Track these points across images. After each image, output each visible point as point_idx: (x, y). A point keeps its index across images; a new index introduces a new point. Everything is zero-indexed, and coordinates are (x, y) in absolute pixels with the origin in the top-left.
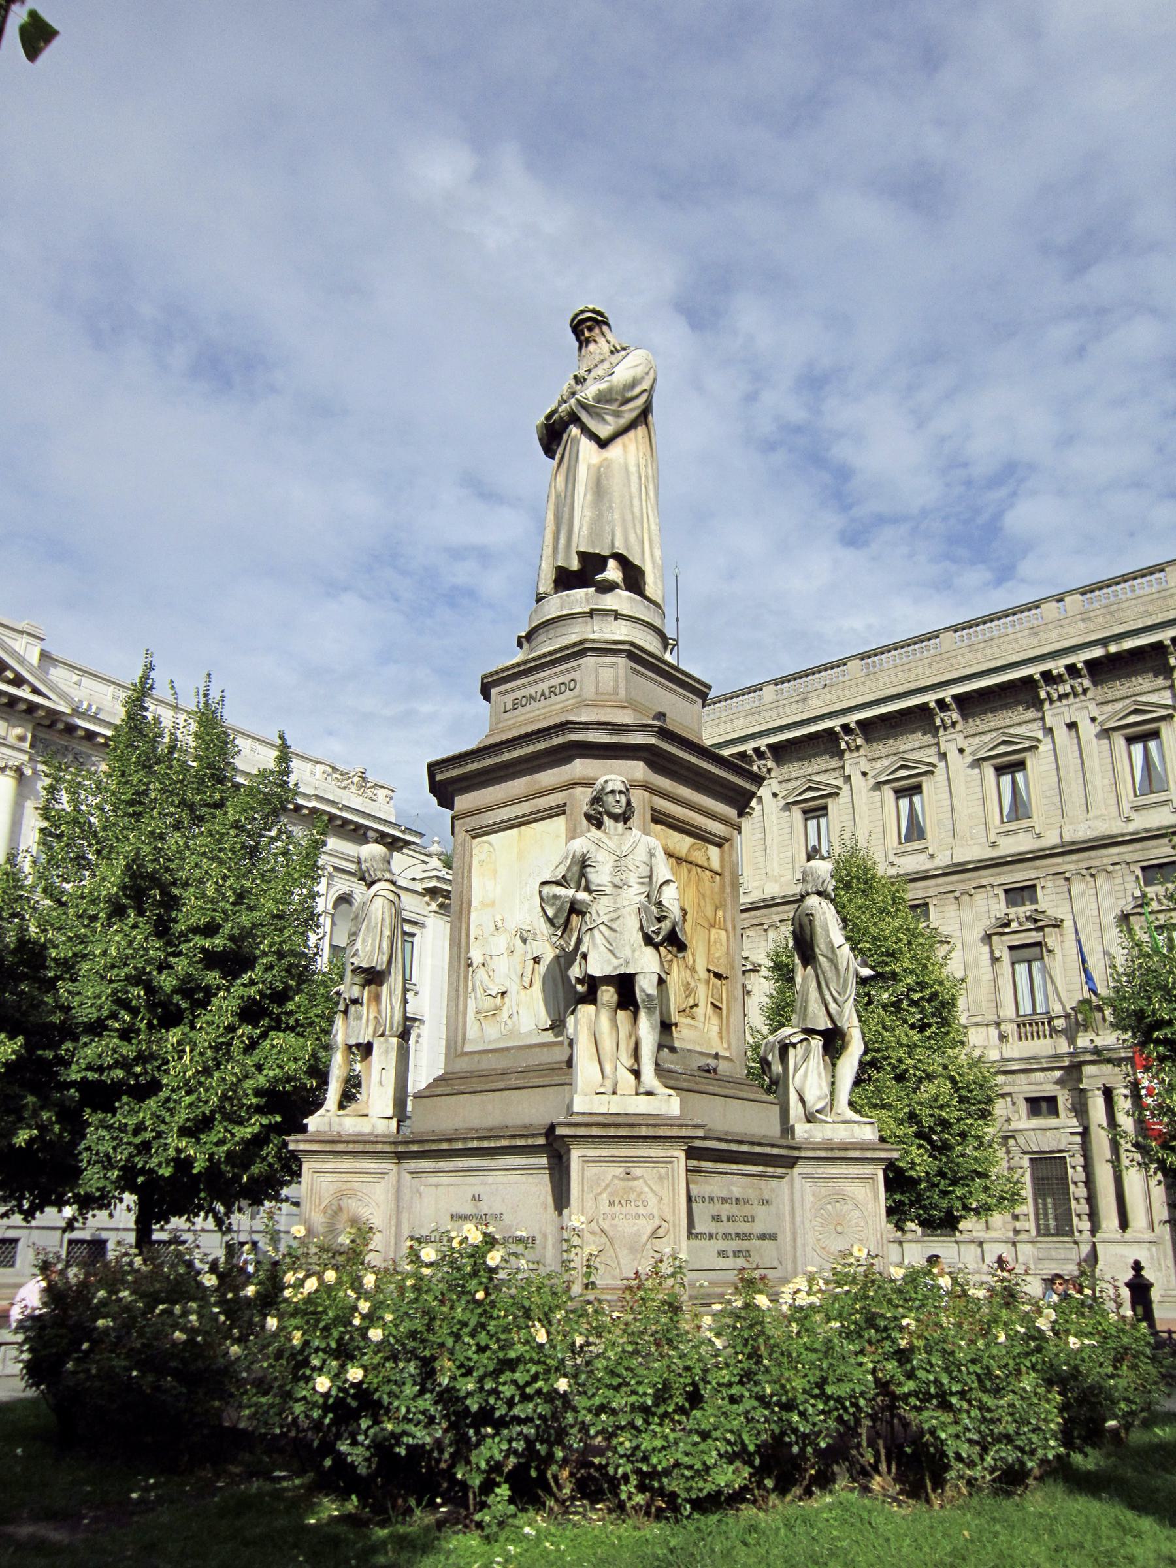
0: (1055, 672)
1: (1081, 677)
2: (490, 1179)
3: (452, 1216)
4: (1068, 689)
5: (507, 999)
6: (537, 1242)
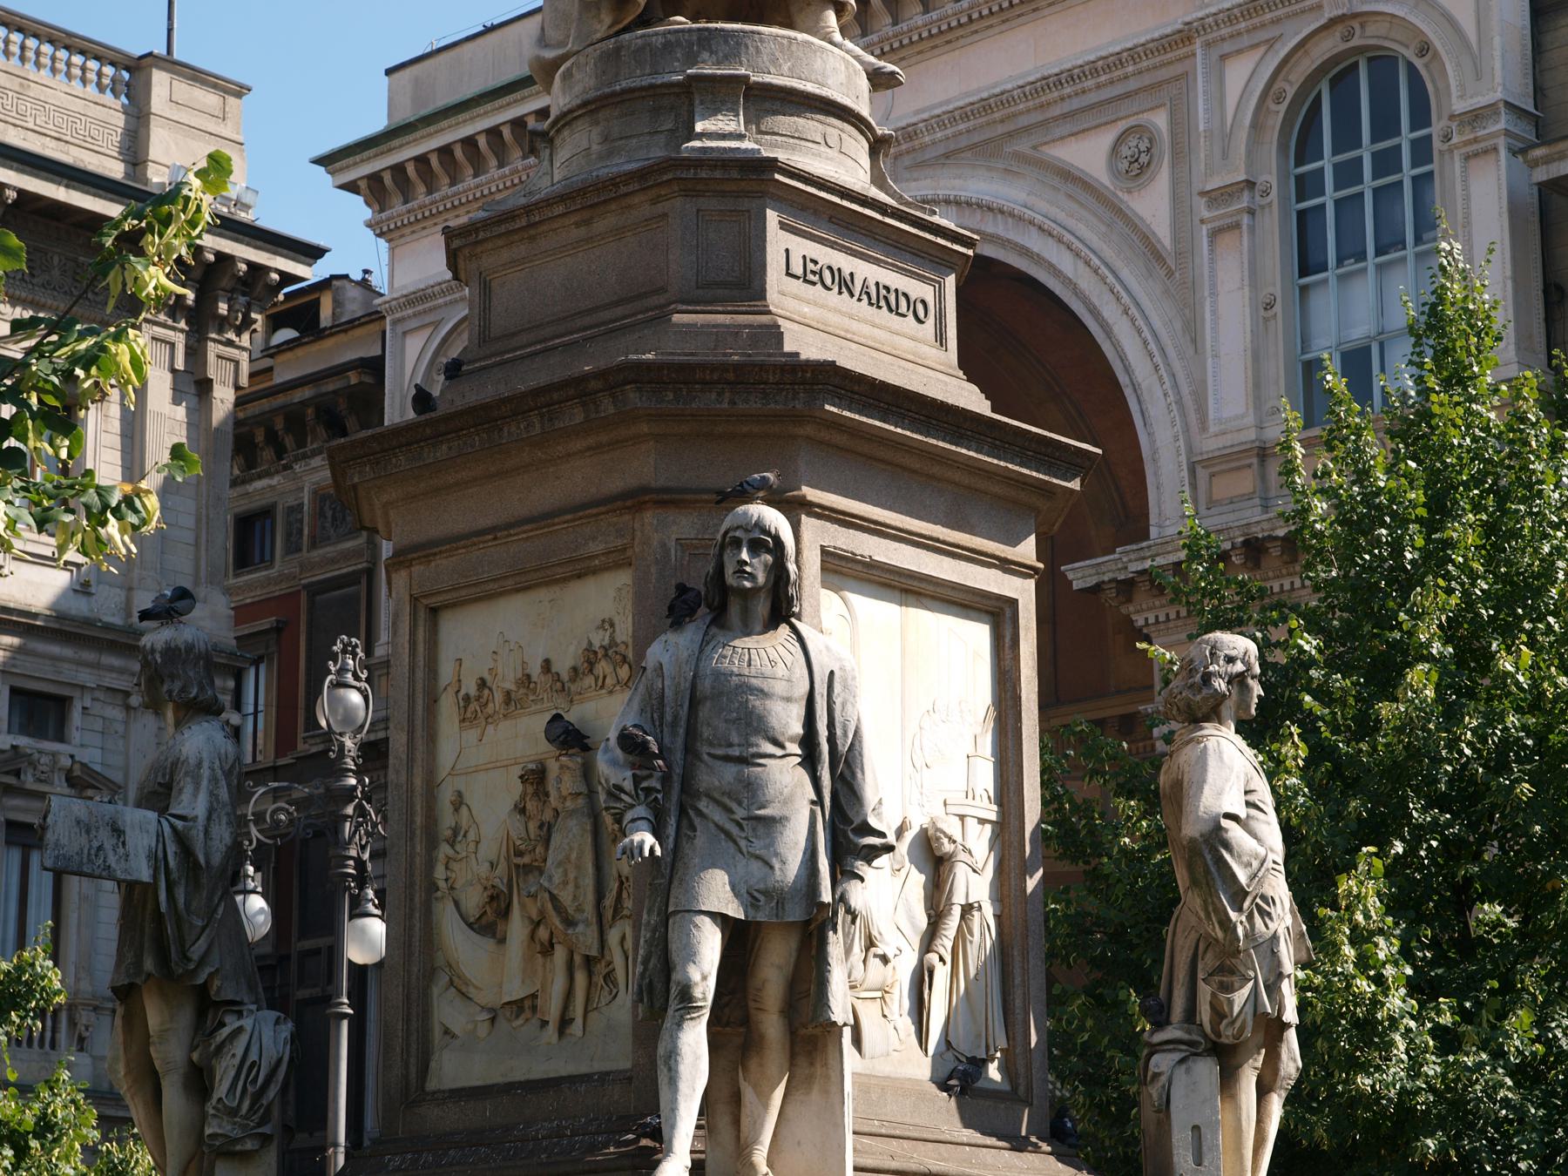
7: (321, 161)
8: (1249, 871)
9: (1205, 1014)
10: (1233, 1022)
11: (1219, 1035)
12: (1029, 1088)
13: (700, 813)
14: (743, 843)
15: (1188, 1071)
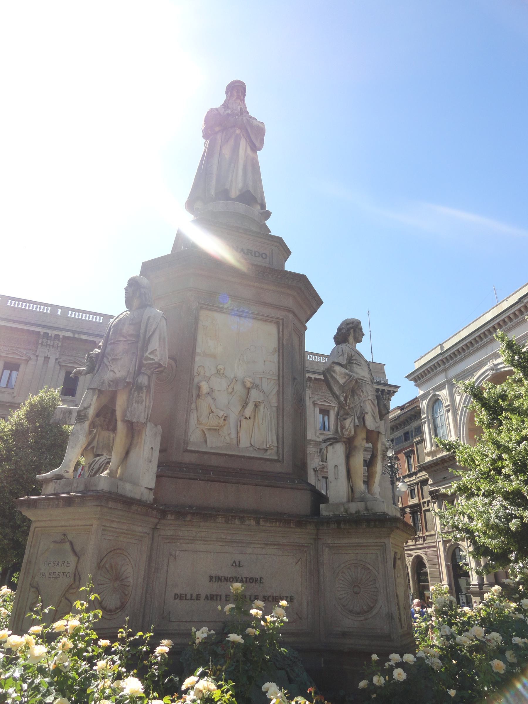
0: (50, 335)
1: (59, 341)
2: (249, 551)
3: (211, 578)
4: (51, 344)
5: (226, 422)
6: (295, 601)
7: (407, 377)
8: (345, 380)
9: (339, 430)
10: (347, 430)
11: (343, 434)
12: (283, 457)
13: (104, 362)
14: (109, 367)
15: (333, 448)
